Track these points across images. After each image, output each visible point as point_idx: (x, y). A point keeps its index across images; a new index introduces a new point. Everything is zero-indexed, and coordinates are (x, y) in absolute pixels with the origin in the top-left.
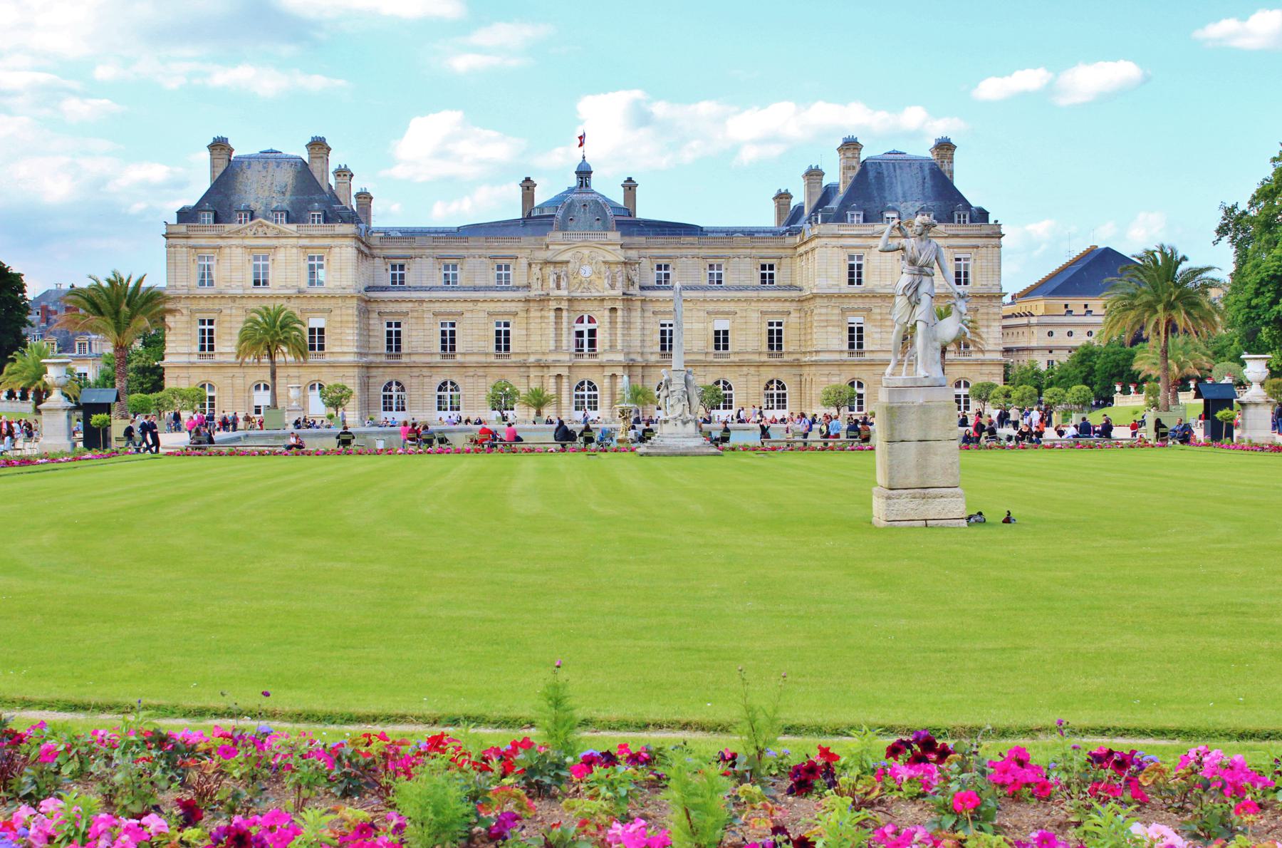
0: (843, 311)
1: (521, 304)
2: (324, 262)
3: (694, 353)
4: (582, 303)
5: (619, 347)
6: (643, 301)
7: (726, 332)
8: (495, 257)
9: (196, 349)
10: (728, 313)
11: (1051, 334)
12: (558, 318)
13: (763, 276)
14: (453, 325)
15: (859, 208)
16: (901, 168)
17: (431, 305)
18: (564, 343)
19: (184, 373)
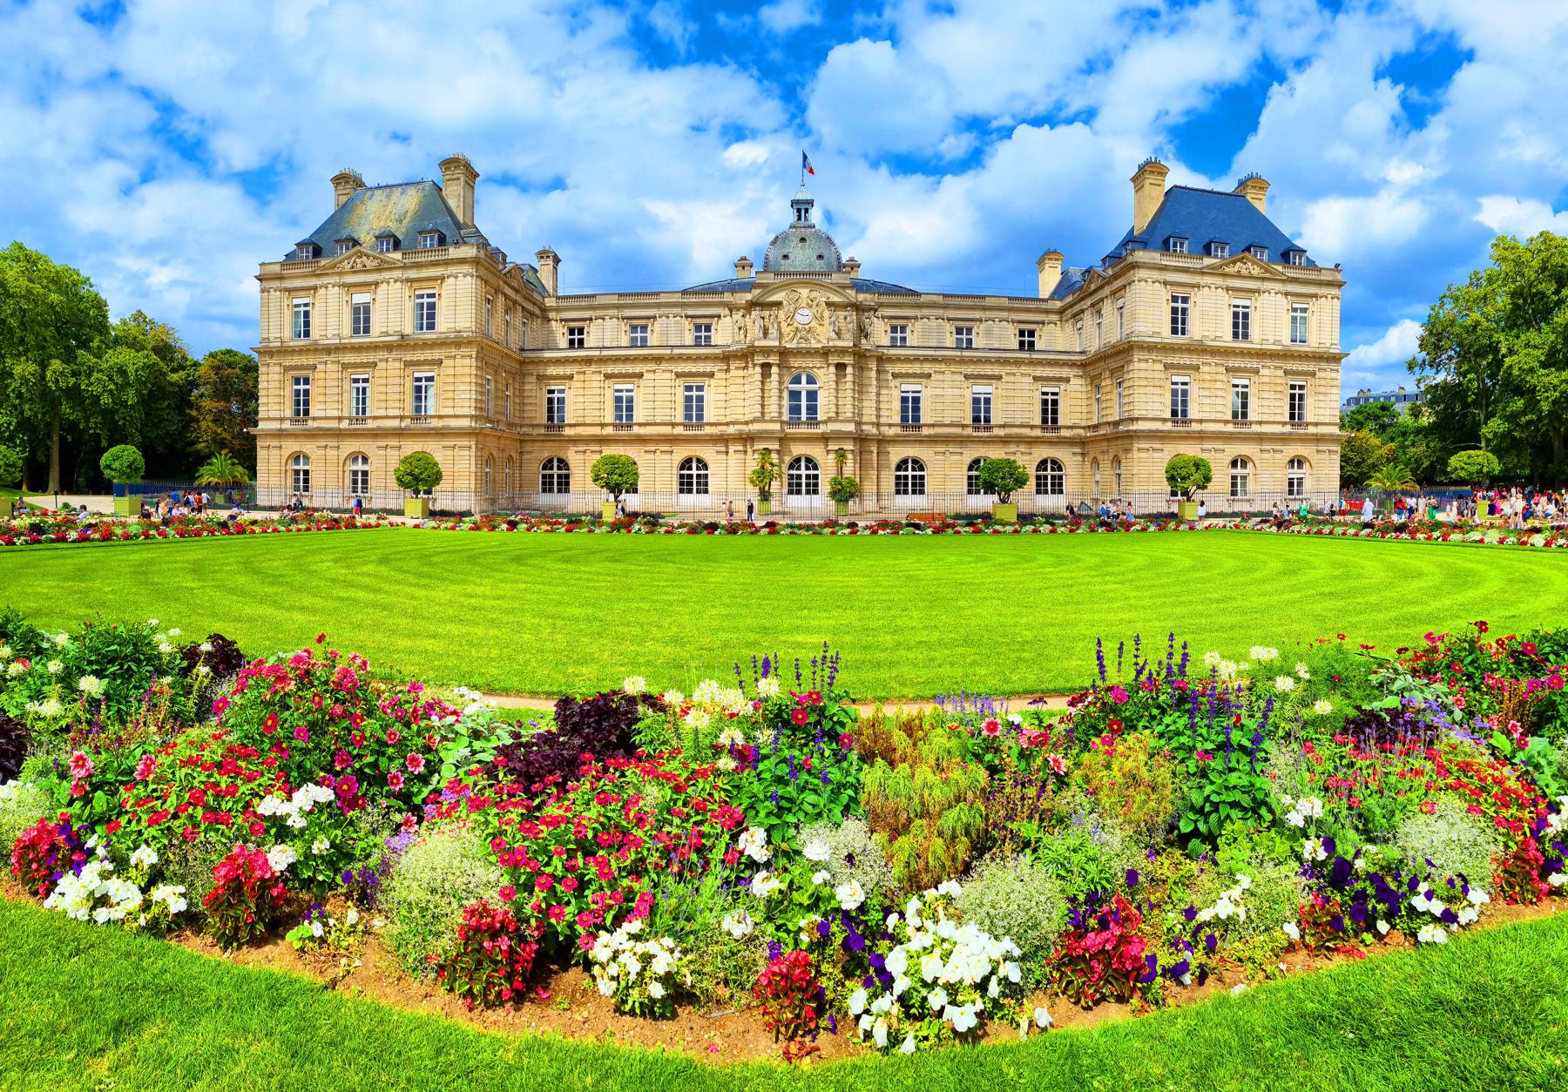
0: (1167, 367)
6: (881, 360)
7: (987, 401)
8: (693, 317)
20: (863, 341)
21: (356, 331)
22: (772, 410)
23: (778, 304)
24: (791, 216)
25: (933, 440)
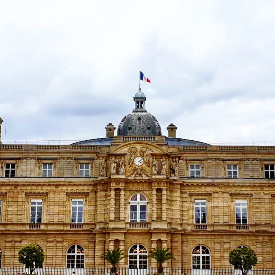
1: (91, 187)
3: (220, 225)
4: (135, 185)
5: (163, 219)
6: (182, 185)
12: (118, 196)
13: (267, 173)
17: (25, 188)
18: (122, 215)
20: (173, 175)
23: (124, 155)
24: (133, 105)
25: (214, 233)
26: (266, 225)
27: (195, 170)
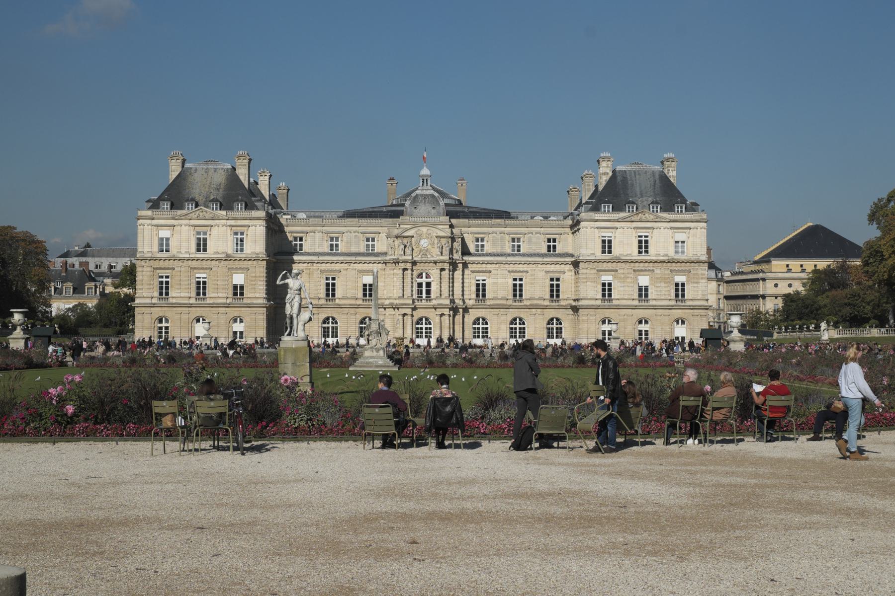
2: (244, 236)
8: (365, 233)
9: (156, 294)
10: (522, 272)
11: (776, 285)
13: (549, 247)
14: (334, 279)
15: (609, 202)
16: (639, 174)
19: (148, 310)
21: (198, 250)
22: (408, 293)
25: (492, 307)
26: (540, 299)
27: (480, 243)
